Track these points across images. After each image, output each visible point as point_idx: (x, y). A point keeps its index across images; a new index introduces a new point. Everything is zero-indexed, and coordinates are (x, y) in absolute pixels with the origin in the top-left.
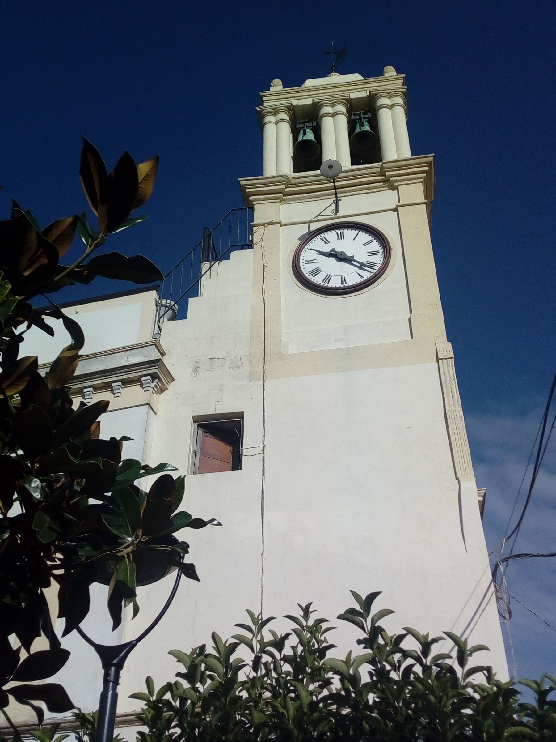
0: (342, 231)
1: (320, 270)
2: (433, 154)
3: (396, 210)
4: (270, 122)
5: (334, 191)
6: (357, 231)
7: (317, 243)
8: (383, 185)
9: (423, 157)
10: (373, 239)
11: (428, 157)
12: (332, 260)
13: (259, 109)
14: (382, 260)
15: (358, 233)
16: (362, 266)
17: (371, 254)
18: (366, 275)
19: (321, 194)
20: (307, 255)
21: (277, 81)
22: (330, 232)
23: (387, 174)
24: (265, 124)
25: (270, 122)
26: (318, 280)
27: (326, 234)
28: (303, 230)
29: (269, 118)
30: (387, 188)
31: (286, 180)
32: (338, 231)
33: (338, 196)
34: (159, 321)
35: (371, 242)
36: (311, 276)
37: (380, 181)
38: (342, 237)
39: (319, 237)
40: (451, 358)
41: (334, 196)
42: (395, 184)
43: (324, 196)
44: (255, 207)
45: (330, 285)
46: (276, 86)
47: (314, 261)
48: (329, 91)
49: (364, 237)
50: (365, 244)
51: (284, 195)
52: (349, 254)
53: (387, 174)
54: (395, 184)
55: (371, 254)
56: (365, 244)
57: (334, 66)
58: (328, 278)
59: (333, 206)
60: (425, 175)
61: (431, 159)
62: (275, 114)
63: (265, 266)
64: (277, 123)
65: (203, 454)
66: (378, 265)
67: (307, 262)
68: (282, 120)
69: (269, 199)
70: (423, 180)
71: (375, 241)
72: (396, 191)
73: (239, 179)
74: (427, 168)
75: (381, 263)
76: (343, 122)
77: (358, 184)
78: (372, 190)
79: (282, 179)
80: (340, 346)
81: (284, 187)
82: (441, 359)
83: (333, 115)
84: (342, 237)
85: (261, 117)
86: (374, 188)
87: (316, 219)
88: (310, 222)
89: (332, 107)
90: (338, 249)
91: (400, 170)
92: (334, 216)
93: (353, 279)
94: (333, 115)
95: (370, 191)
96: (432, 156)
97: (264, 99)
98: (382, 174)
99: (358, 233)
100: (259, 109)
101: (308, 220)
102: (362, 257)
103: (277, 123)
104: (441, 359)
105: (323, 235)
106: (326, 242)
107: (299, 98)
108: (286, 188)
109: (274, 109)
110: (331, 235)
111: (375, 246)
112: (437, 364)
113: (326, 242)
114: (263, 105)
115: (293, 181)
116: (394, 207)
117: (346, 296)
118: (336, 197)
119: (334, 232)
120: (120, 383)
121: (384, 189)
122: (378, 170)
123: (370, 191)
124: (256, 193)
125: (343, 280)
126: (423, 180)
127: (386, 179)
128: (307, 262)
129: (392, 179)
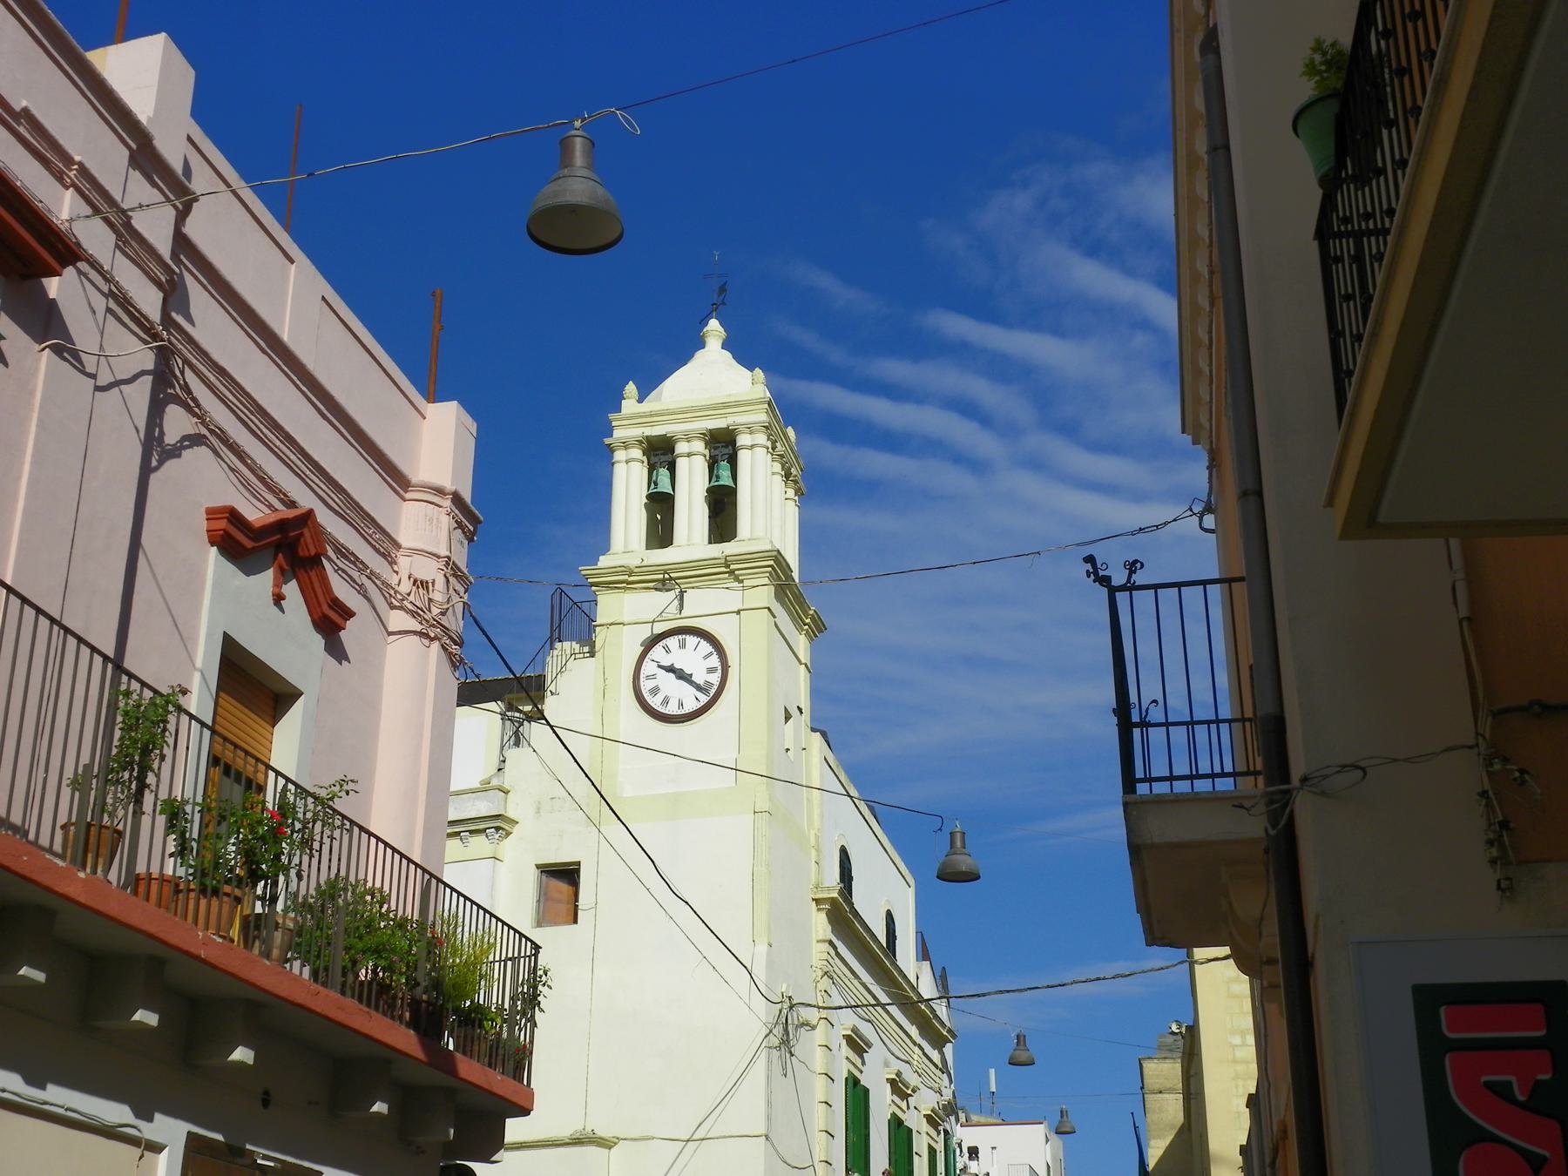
0: (684, 636)
3: (738, 612)
4: (618, 462)
7: (657, 652)
12: (672, 676)
13: (607, 441)
14: (719, 680)
16: (699, 688)
17: (711, 670)
18: (704, 699)
20: (648, 667)
21: (631, 388)
24: (613, 464)
25: (618, 462)
26: (655, 702)
27: (668, 639)
28: (645, 633)
29: (620, 455)
32: (680, 637)
34: (502, 749)
35: (711, 654)
36: (651, 697)
38: (683, 645)
42: (740, 578)
44: (599, 598)
45: (667, 712)
46: (629, 398)
47: (653, 677)
48: (685, 416)
49: (706, 647)
50: (706, 657)
53: (732, 567)
56: (706, 657)
57: (715, 304)
58: (666, 701)
59: (676, 602)
62: (626, 448)
64: (627, 462)
65: (547, 900)
67: (648, 678)
68: (633, 460)
70: (768, 575)
73: (580, 568)
75: (718, 683)
76: (700, 465)
79: (623, 568)
83: (689, 455)
84: (683, 645)
85: (610, 450)
86: (719, 579)
87: (659, 619)
88: (653, 622)
89: (688, 441)
90: (677, 666)
92: (678, 616)
93: (691, 706)
94: (689, 455)
97: (614, 424)
98: (728, 566)
100: (607, 441)
101: (651, 620)
102: (699, 678)
103: (627, 462)
106: (668, 651)
107: (652, 424)
109: (624, 443)
111: (714, 661)
113: (668, 651)
114: (612, 436)
115: (636, 570)
119: (676, 637)
120: (467, 833)
122: (723, 561)
125: (681, 704)
126: (768, 575)
128: (648, 678)
129: (736, 572)
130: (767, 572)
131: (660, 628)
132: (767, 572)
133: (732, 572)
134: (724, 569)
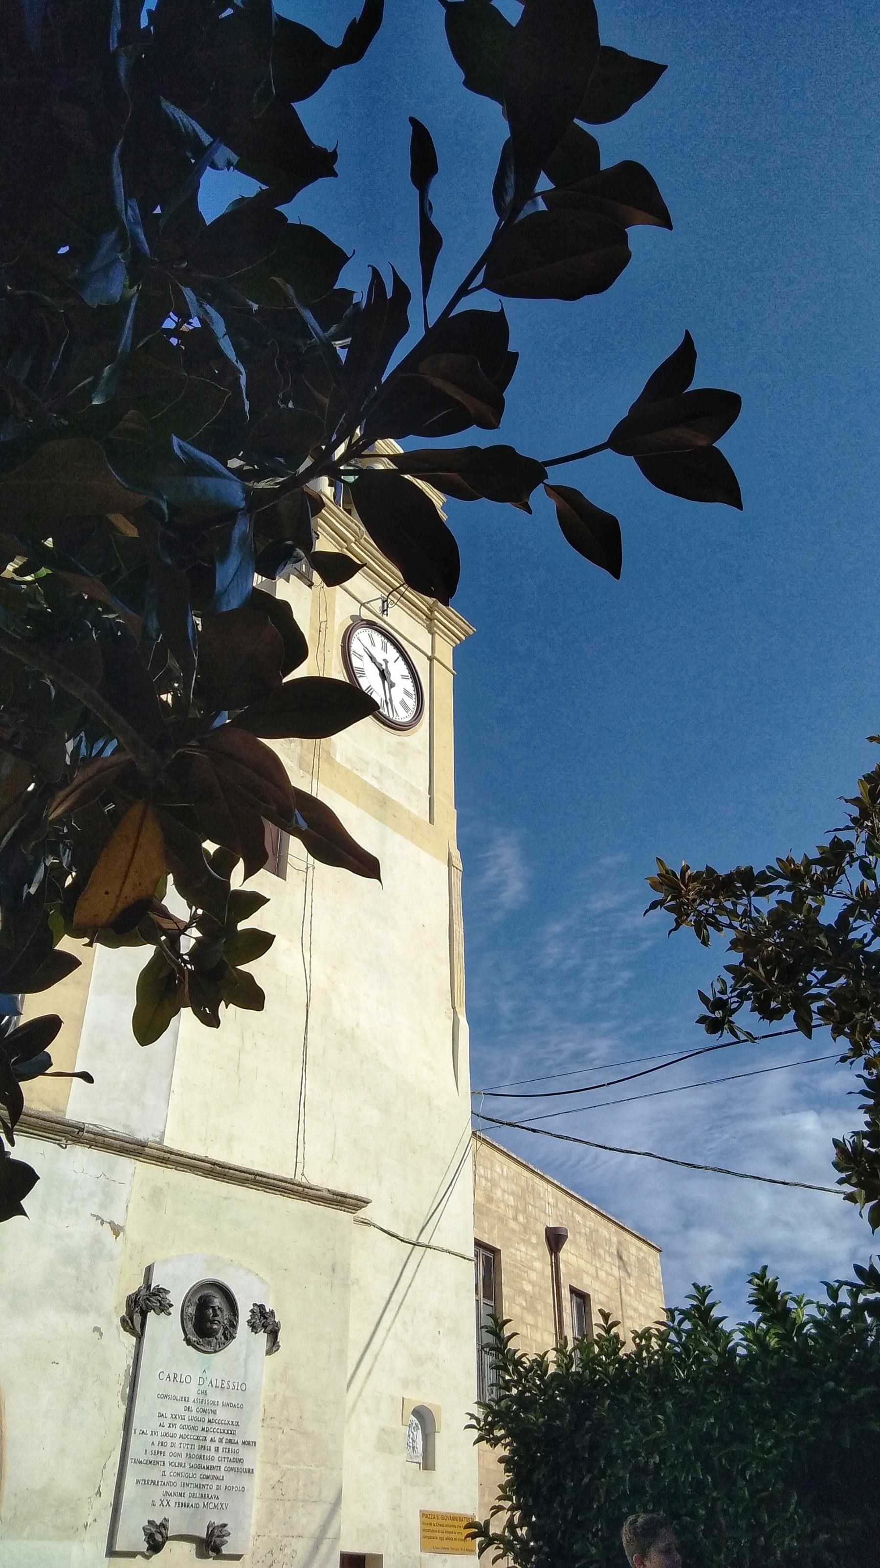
1: (364, 674)
2: (475, 630)
5: (391, 590)
6: (398, 655)
8: (426, 619)
9: (468, 625)
10: (409, 675)
11: (471, 628)
15: (398, 658)
19: (376, 579)
22: (377, 633)
23: (436, 613)
30: (425, 625)
31: (359, 535)
32: (383, 638)
33: (390, 596)
37: (424, 612)
39: (368, 629)
40: (460, 871)
41: (387, 594)
42: (435, 629)
43: (376, 582)
51: (346, 548)
52: (393, 678)
54: (435, 629)
55: (406, 692)
60: (458, 642)
61: (471, 632)
63: (323, 626)
66: (410, 712)
69: (333, 538)
70: (454, 645)
71: (411, 680)
72: (430, 636)
74: (464, 638)
77: (410, 601)
78: (414, 616)
80: (374, 783)
81: (353, 539)
82: (454, 866)
86: (417, 615)
88: (363, 604)
91: (445, 619)
92: (381, 615)
95: (412, 615)
96: (473, 631)
99: (398, 658)
104: (454, 866)
105: (370, 631)
106: (373, 644)
108: (355, 543)
110: (378, 638)
112: (447, 868)
113: (373, 644)
115: (362, 541)
116: (430, 654)
117: (382, 725)
118: (388, 596)
119: (380, 635)
121: (424, 624)
123: (412, 615)
124: (327, 521)
127: (430, 617)
129: (436, 621)
130: (455, 643)
131: (366, 615)
132: (455, 643)
133: (430, 619)
134: (426, 609)
